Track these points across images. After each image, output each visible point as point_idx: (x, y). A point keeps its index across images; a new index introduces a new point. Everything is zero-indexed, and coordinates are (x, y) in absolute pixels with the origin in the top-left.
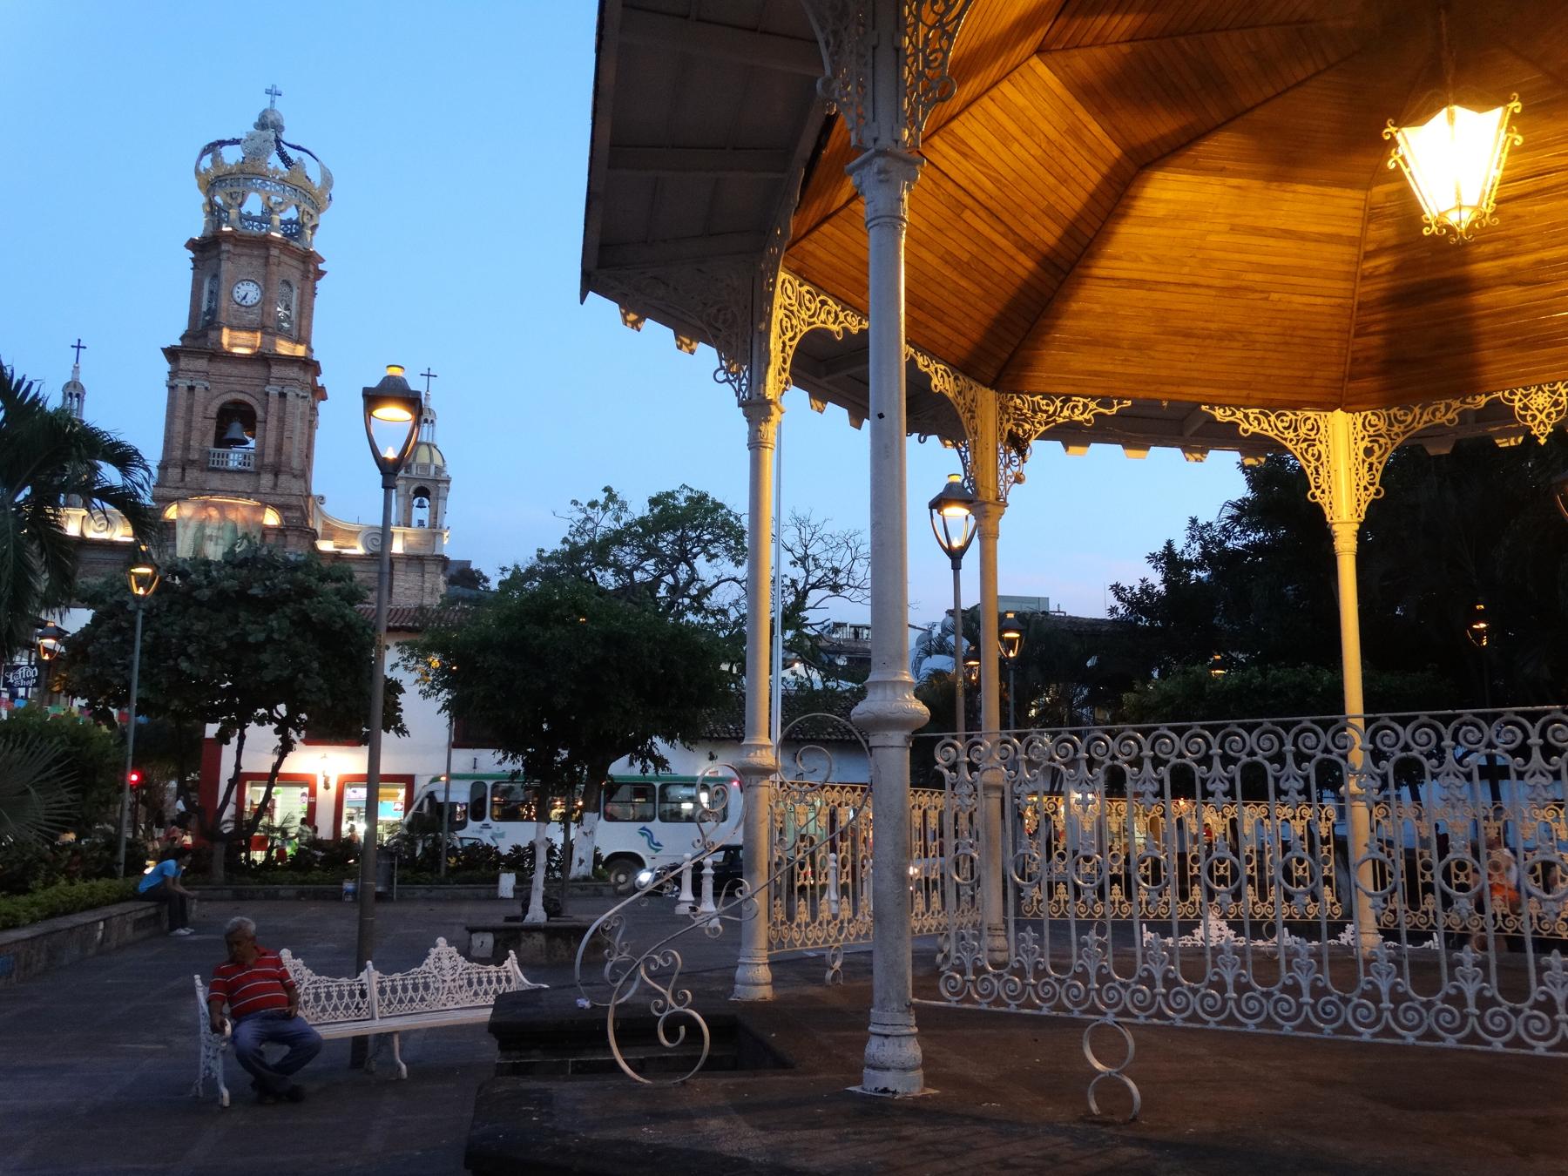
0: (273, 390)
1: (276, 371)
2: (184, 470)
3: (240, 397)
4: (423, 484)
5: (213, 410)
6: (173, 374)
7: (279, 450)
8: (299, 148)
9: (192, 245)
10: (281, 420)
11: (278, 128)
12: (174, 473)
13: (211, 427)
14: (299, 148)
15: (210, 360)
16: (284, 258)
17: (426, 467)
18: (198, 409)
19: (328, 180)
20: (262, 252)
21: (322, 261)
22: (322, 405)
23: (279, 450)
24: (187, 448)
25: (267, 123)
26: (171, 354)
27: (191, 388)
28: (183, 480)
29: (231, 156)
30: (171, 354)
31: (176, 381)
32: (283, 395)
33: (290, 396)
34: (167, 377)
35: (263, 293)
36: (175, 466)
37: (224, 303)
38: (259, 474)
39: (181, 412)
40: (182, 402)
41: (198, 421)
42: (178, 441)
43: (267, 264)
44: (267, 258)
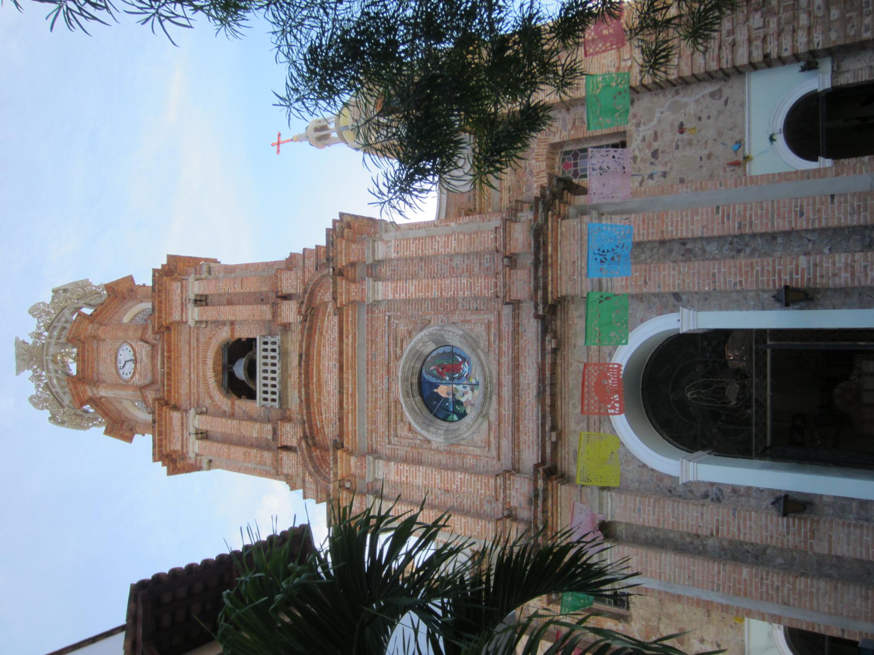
3: (210, 363)
5: (223, 401)
12: (289, 461)
27: (203, 435)
30: (174, 462)
32: (201, 301)
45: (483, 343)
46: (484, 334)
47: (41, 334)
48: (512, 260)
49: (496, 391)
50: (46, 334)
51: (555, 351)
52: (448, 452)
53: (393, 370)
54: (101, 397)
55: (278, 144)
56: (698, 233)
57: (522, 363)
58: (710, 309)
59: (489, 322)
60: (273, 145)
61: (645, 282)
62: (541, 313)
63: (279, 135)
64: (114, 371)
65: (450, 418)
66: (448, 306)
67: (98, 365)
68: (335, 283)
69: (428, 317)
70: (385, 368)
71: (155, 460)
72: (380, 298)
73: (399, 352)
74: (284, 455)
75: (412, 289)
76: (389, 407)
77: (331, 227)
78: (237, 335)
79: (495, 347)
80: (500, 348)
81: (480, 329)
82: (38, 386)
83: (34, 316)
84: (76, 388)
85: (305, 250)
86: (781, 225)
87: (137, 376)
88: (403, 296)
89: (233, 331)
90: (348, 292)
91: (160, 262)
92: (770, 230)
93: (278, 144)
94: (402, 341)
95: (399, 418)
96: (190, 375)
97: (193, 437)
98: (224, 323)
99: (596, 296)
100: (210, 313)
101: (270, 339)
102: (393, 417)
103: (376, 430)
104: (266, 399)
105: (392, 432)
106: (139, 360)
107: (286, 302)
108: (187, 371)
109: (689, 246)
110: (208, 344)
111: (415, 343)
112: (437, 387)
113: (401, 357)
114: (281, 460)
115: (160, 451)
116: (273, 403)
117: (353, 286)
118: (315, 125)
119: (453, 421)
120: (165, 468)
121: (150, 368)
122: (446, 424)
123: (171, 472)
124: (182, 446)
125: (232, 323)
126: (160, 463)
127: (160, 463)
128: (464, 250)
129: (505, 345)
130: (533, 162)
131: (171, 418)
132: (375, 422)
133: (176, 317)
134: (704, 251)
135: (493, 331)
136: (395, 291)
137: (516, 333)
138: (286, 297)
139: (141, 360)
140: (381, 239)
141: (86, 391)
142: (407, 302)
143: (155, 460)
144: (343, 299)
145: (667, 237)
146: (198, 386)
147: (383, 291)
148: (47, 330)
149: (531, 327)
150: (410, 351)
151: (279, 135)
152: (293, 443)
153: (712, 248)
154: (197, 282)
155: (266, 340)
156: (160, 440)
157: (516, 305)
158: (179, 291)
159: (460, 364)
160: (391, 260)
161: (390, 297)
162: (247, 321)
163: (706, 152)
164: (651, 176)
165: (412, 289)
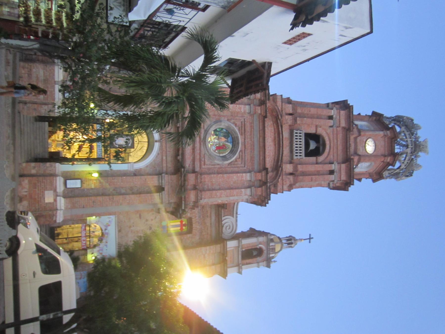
4: (265, 252)
7: (304, 174)
10: (318, 173)
12: (289, 108)
13: (312, 130)
17: (274, 249)
20: (387, 153)
23: (304, 174)
24: (302, 116)
27: (331, 118)
32: (332, 172)
33: (332, 177)
36: (293, 109)
38: (291, 163)
42: (305, 111)
43: (385, 156)
45: (207, 157)
46: (206, 161)
47: (415, 157)
48: (195, 188)
49: (202, 140)
50: (413, 157)
51: (178, 155)
52: (220, 116)
53: (243, 147)
54: (383, 131)
55: (310, 238)
56: (127, 196)
57: (192, 150)
58: (124, 170)
59: (204, 165)
60: (312, 238)
61: (146, 180)
62: (183, 169)
63: (310, 242)
64: (376, 142)
65: (220, 129)
66: (221, 172)
67: (385, 144)
68: (267, 179)
69: (229, 166)
70: (246, 147)
71: (352, 106)
72: (248, 174)
73: (241, 153)
74: (291, 112)
75: (235, 177)
76: (245, 133)
77: (269, 201)
78: (315, 158)
79: (202, 156)
80: (200, 156)
81: (207, 162)
82: (416, 134)
83: (418, 165)
84: (395, 135)
85: (283, 193)
86: (100, 198)
87: (365, 140)
88: (239, 175)
89: (317, 161)
90: (262, 176)
91: (351, 188)
92: (104, 197)
93: (310, 238)
94: (239, 158)
95: (240, 129)
96: (337, 142)
97: (334, 116)
98: (321, 163)
99: (163, 175)
100: (328, 167)
101: (299, 157)
102: (243, 129)
103: (250, 123)
104: (300, 133)
105: (243, 123)
107: (291, 172)
108: (339, 143)
109: (131, 192)
110: (328, 154)
111: (233, 157)
112: (225, 141)
113: (240, 152)
114: (292, 110)
115: (350, 110)
116: (297, 132)
117: (260, 178)
118: (293, 245)
119: (219, 128)
120: (348, 103)
121: (358, 144)
122: (222, 127)
123: (347, 101)
124: (340, 112)
125: (317, 163)
126: (350, 105)
127: (350, 105)
128: (214, 192)
129: (198, 157)
130: (198, 227)
131: (346, 123)
132: (251, 126)
133: (343, 166)
134: (126, 190)
135: (203, 162)
136: (242, 177)
137: (194, 161)
138: (291, 174)
139: (362, 147)
140: (249, 196)
141: (391, 133)
142: (237, 172)
143: (352, 106)
144: (264, 173)
145: (138, 195)
146: (333, 138)
147: (247, 177)
148: (412, 159)
149: (188, 163)
150: (236, 154)
151: (310, 242)
152: (287, 117)
153: (123, 191)
154: (333, 179)
155: (300, 157)
156: (350, 115)
157: (194, 172)
159: (216, 150)
160: (244, 188)
161: (244, 174)
162: (310, 165)
163: (131, 228)
164: (152, 220)
165: (235, 177)
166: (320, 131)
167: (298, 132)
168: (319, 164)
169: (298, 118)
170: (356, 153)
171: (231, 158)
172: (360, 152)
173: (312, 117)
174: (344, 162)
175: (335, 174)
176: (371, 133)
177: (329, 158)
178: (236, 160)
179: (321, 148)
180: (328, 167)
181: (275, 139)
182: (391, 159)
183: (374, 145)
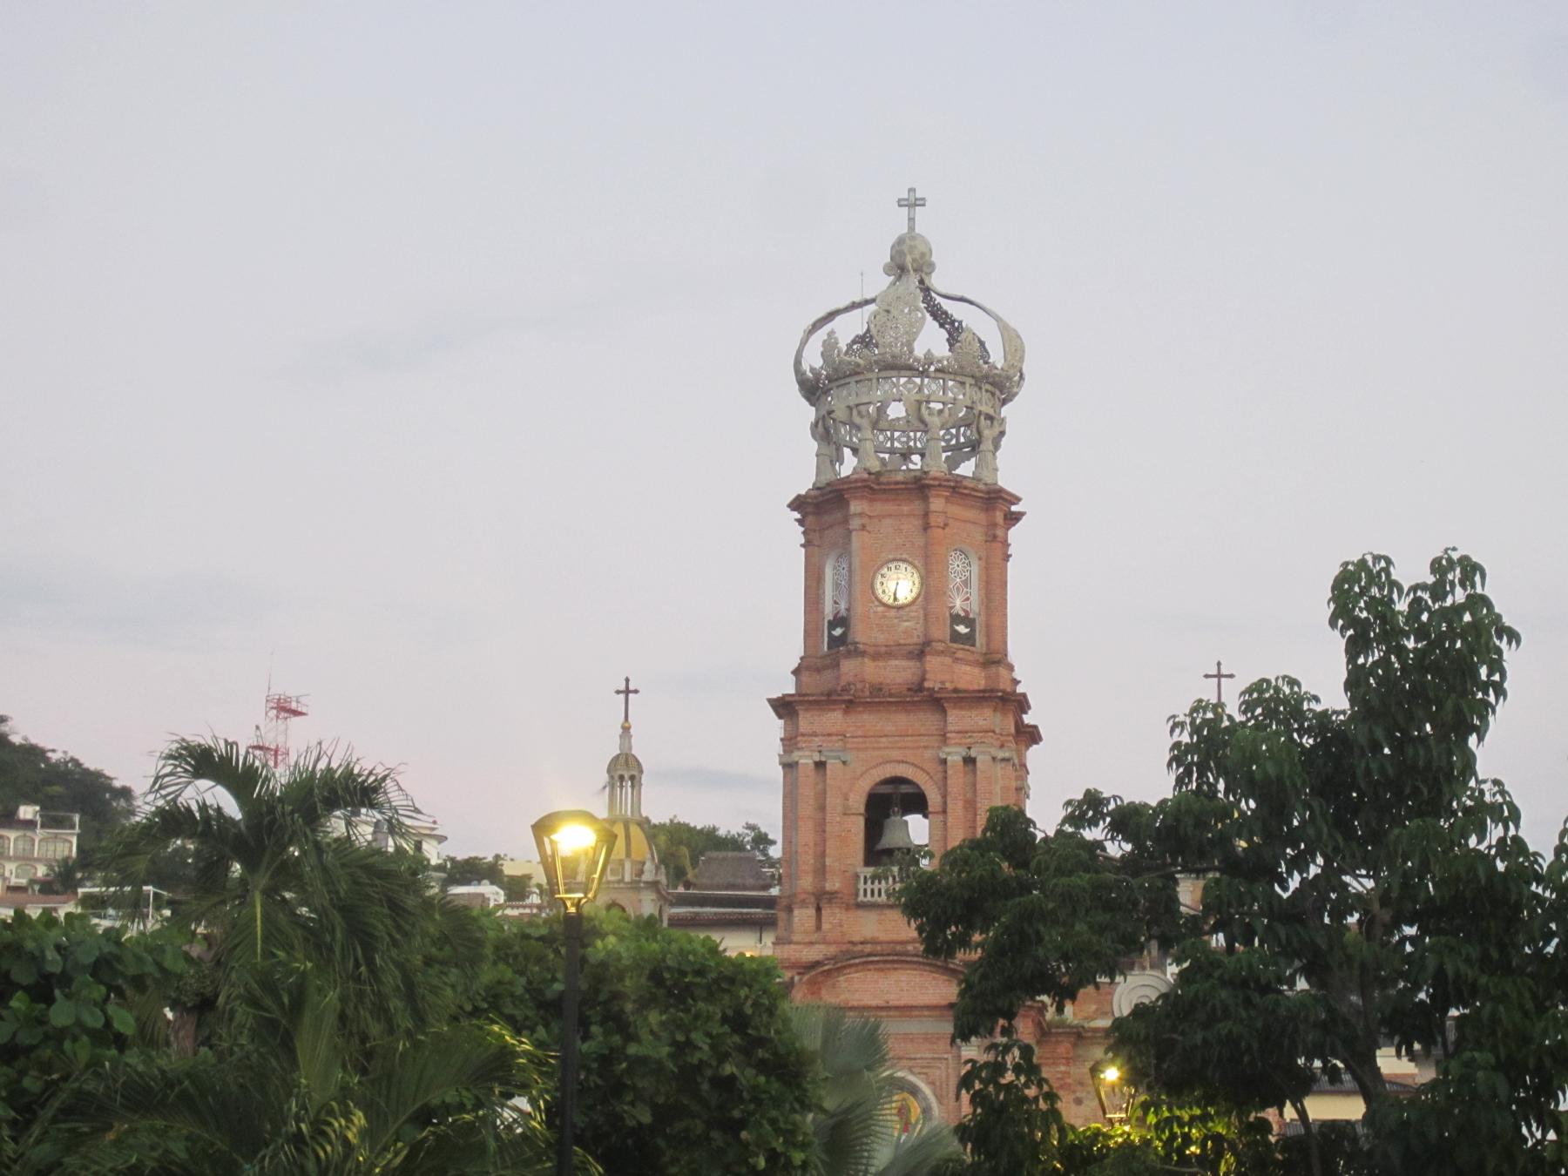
0: (955, 756)
1: (957, 718)
2: (819, 909)
6: (789, 742)
8: (962, 299)
9: (798, 504)
11: (923, 267)
13: (858, 826)
14: (962, 299)
15: (846, 712)
16: (956, 510)
18: (833, 801)
19: (1014, 344)
20: (917, 506)
21: (1017, 500)
22: (1033, 755)
24: (821, 871)
25: (909, 263)
26: (784, 707)
27: (820, 765)
28: (819, 927)
29: (848, 328)
30: (784, 707)
31: (796, 756)
32: (970, 761)
34: (778, 748)
35: (924, 582)
36: (803, 904)
37: (859, 609)
39: (807, 809)
40: (807, 792)
41: (833, 817)
43: (926, 528)
44: (926, 515)
73: (916, 1070)
74: (812, 911)
87: (880, 609)
93: (1219, 676)
98: (944, 797)
100: (957, 779)
106: (901, 612)
108: (890, 728)
125: (944, 812)
152: (825, 926)
154: (988, 758)
158: (981, 723)
166: (858, 802)
167: (861, 886)
168: (945, 803)
169: (828, 887)
170: (920, 652)
171: (925, 1099)
172: (910, 630)
173: (821, 827)
174: (944, 711)
175: (973, 753)
176: (857, 588)
177: (927, 766)
178: (932, 1084)
179: (904, 789)
180: (957, 779)
181: (881, 970)
182: (938, 496)
183: (892, 565)
